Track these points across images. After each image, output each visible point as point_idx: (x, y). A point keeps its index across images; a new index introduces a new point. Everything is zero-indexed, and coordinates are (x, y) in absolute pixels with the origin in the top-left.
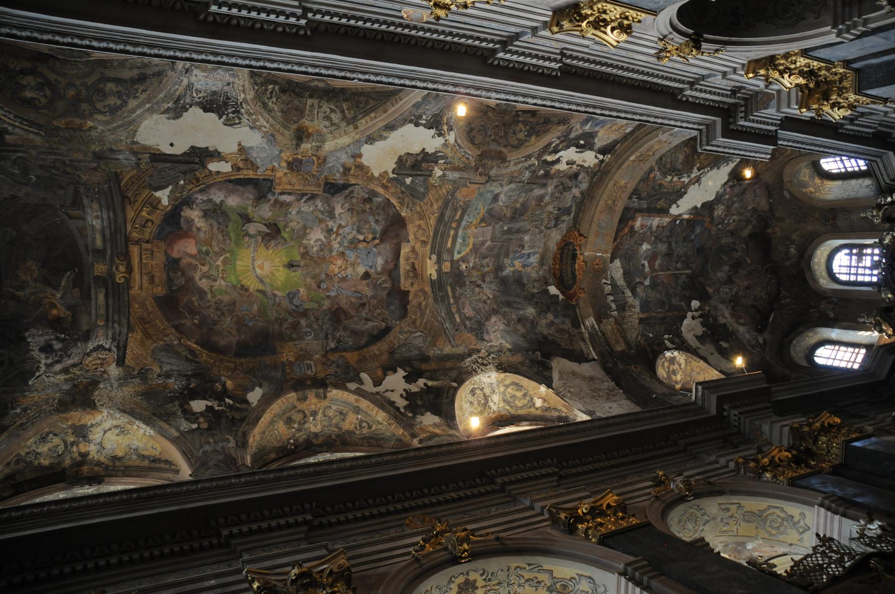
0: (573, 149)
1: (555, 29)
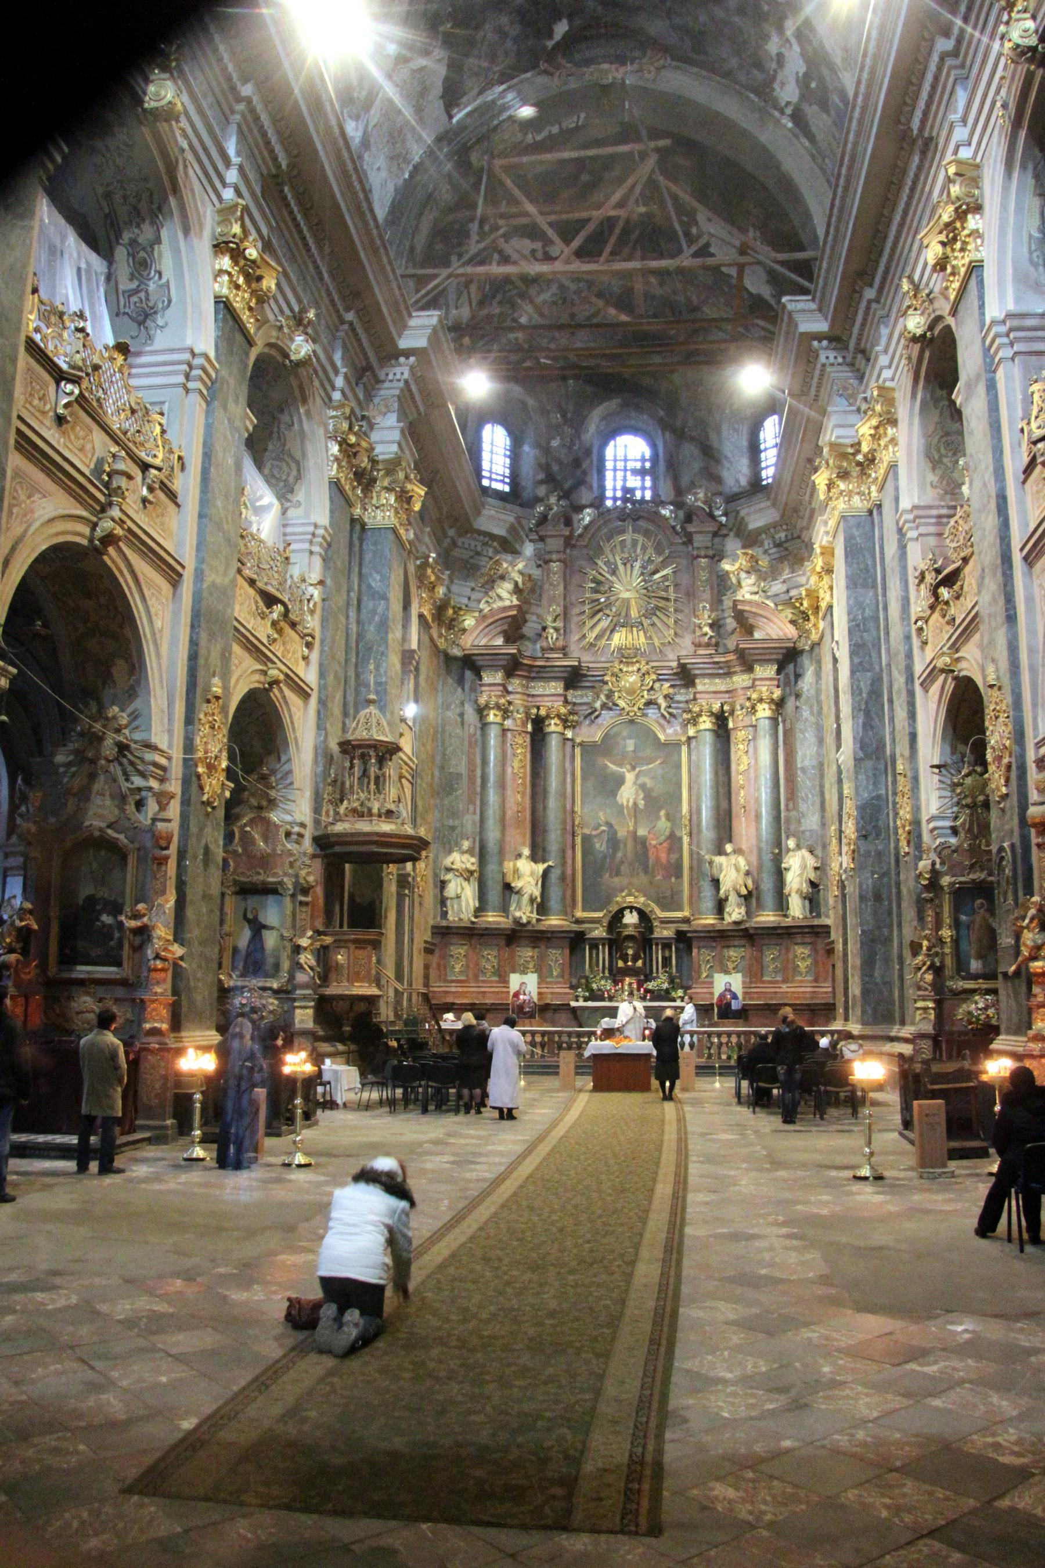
0: (802, 70)
1: (952, 170)
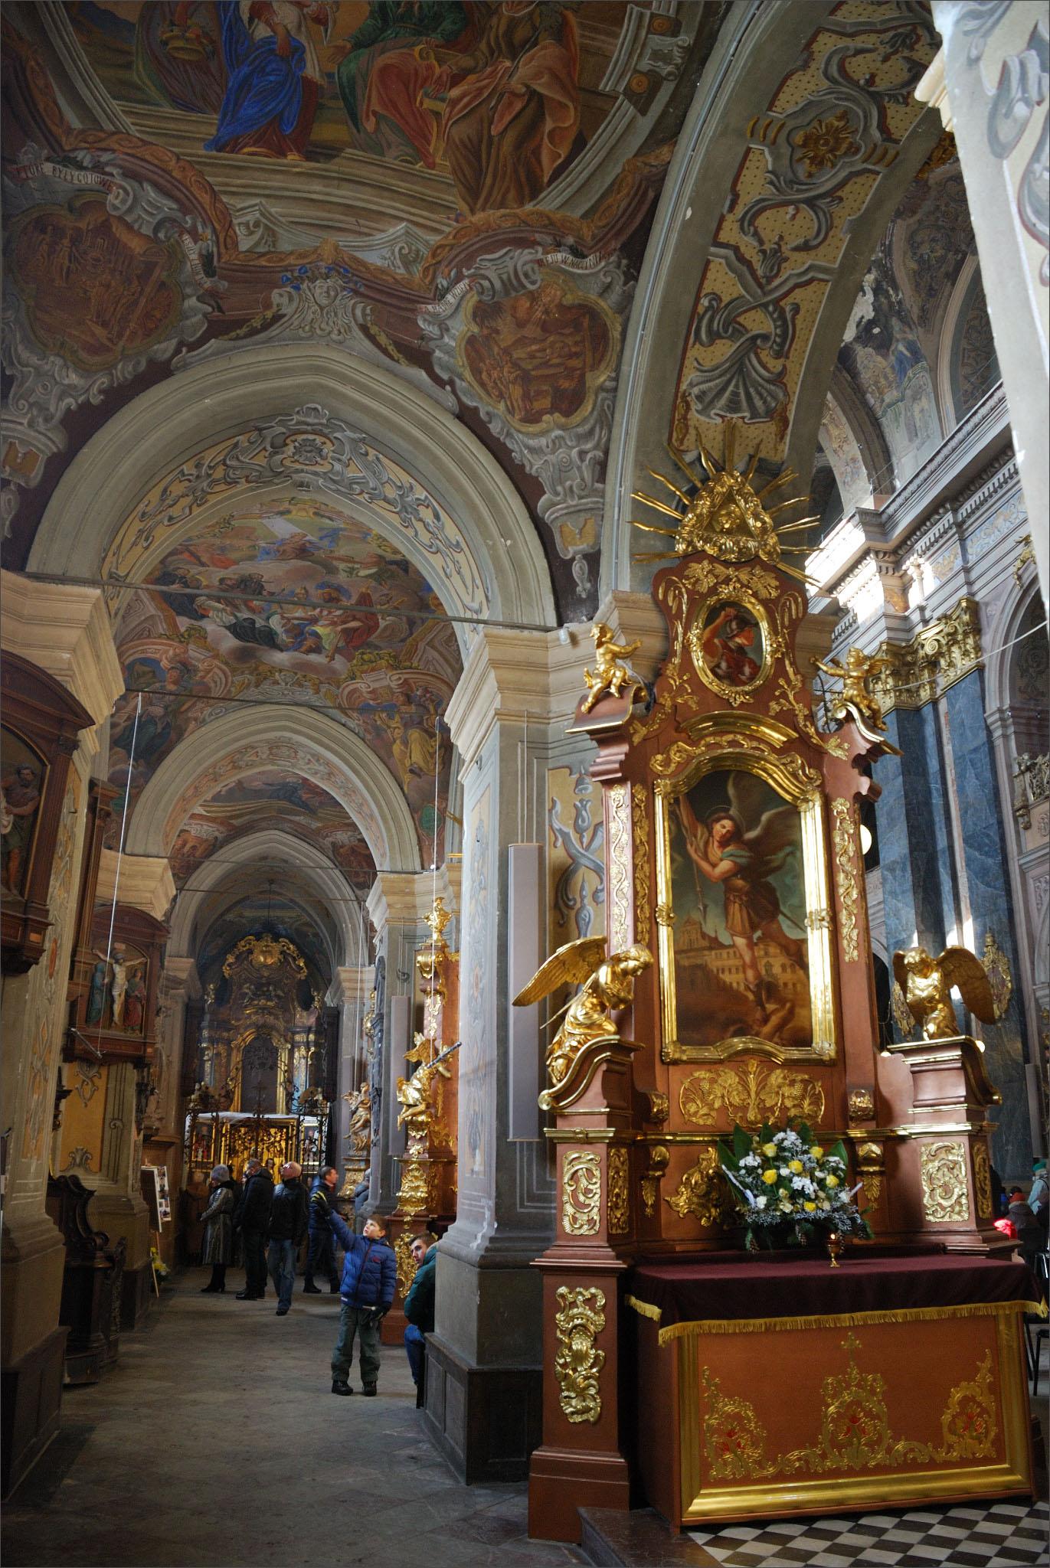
0: (870, 314)
